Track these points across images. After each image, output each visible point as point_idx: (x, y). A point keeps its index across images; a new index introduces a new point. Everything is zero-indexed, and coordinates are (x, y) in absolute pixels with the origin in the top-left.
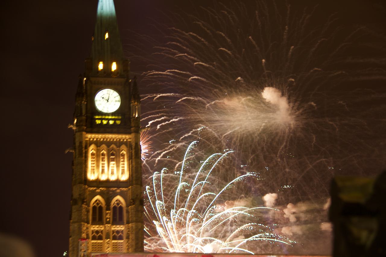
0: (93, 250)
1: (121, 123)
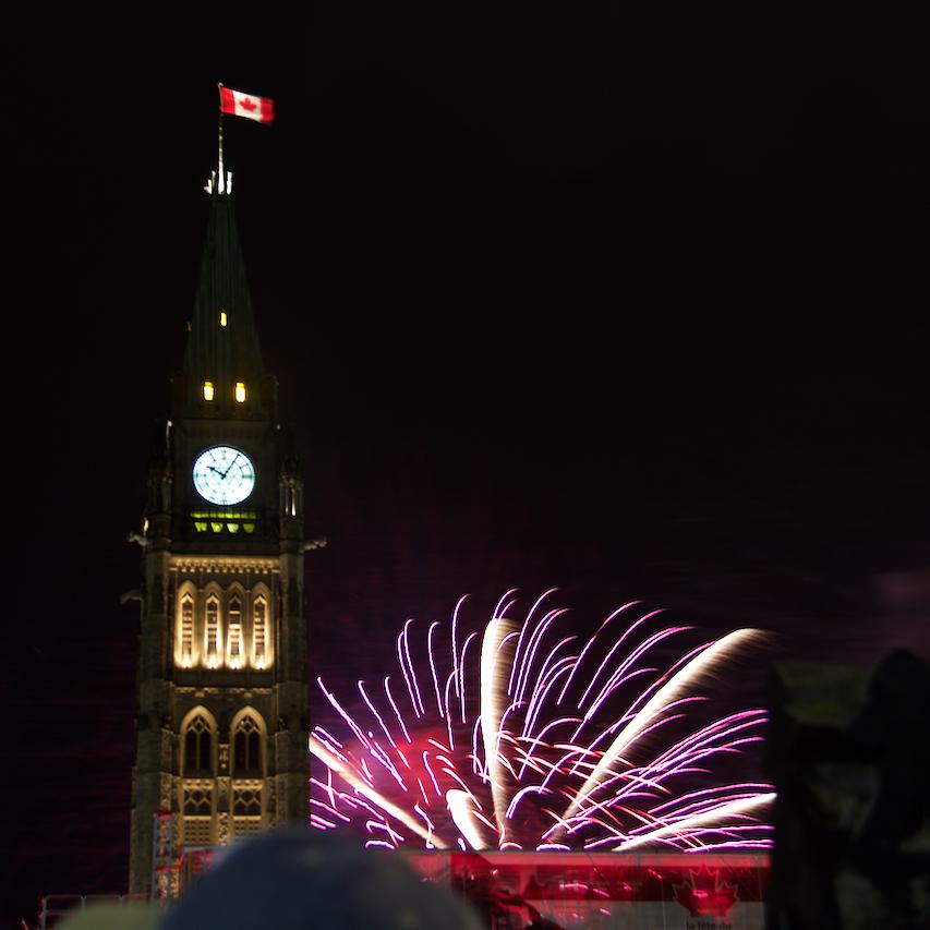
0: (187, 840)
1: (255, 530)
